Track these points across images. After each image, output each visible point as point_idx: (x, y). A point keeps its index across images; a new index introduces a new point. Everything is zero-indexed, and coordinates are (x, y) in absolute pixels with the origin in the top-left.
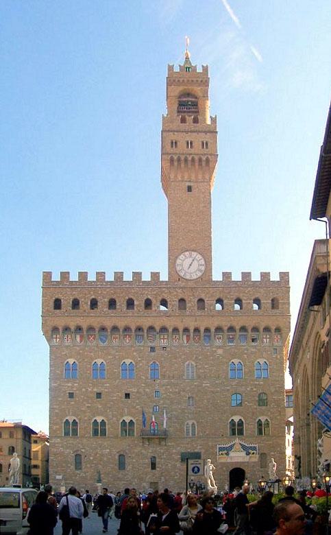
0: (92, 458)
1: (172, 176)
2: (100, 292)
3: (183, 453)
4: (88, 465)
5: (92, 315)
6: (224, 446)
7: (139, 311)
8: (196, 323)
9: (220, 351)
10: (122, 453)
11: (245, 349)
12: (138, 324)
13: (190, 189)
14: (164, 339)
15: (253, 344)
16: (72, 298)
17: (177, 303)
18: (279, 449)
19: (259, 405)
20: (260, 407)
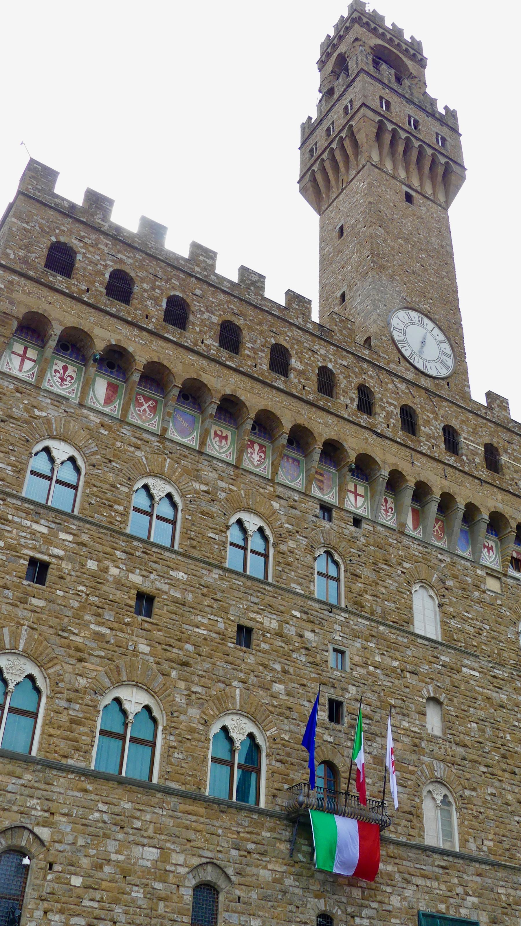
0: (77, 881)
2: (198, 292)
3: (424, 915)
7: (304, 389)
8: (446, 483)
9: (493, 584)
10: (209, 875)
12: (301, 420)
13: (409, 198)
14: (356, 494)
17: (398, 411)
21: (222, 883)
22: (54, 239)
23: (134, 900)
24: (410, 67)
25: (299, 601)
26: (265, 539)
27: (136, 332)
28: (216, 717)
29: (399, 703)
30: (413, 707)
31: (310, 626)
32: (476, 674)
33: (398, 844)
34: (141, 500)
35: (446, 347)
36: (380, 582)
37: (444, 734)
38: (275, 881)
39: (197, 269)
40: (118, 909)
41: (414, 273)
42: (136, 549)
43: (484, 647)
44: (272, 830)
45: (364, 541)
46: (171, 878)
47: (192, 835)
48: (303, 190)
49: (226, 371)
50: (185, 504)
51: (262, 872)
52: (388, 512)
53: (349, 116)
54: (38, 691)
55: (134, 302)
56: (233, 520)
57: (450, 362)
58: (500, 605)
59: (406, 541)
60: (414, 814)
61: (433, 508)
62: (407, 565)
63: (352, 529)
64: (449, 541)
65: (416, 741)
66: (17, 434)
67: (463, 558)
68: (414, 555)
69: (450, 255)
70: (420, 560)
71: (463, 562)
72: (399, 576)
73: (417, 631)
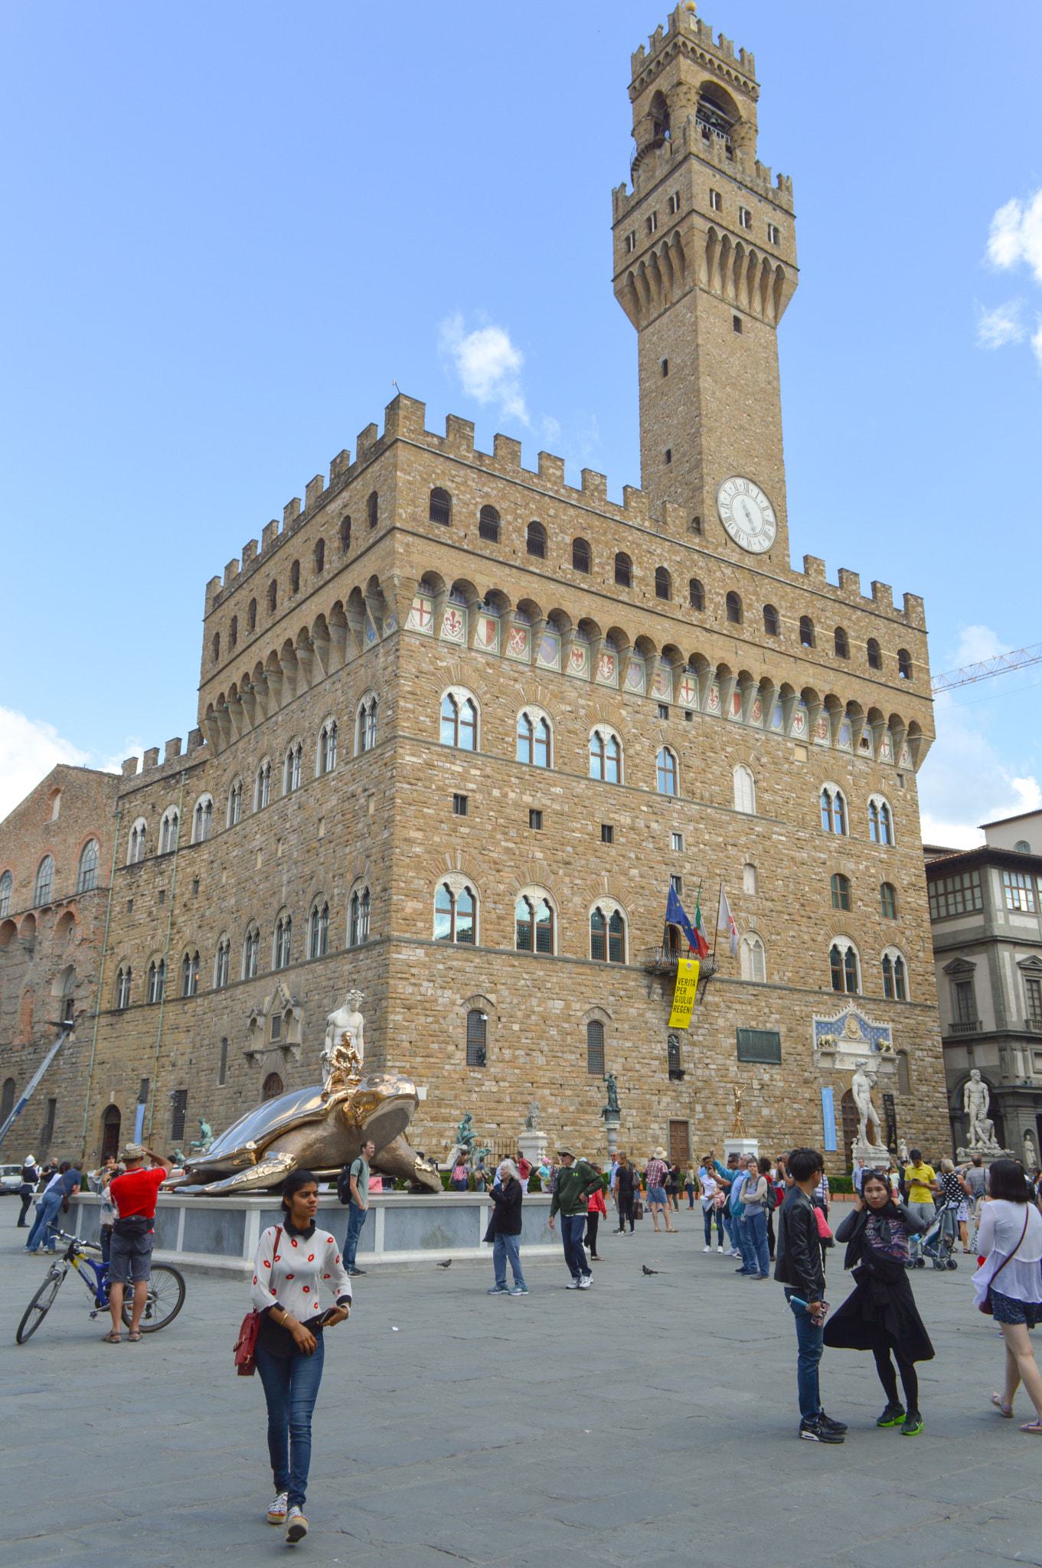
0: (516, 1027)
1: (703, 275)
2: (552, 512)
4: (506, 1052)
5: (532, 569)
6: (826, 1019)
8: (765, 667)
9: (800, 754)
10: (597, 1015)
11: (849, 762)
14: (688, 689)
15: (862, 751)
16: (481, 502)
18: (929, 1043)
19: (886, 915)
20: (885, 921)
21: (605, 1020)
22: (432, 487)
23: (552, 1036)
24: (740, 106)
25: (646, 797)
26: (617, 744)
27: (507, 570)
28: (591, 902)
29: (723, 872)
31: (654, 817)
33: (722, 981)
34: (522, 729)
35: (769, 515)
37: (757, 892)
38: (640, 1015)
39: (549, 485)
40: (543, 1043)
41: (741, 427)
42: (524, 773)
44: (635, 980)
46: (573, 1019)
47: (584, 989)
48: (619, 294)
49: (580, 593)
50: (555, 726)
51: (632, 1010)
53: (677, 218)
54: (472, 897)
55: (503, 537)
56: (592, 733)
57: (772, 531)
59: (729, 727)
60: (734, 957)
61: (754, 693)
62: (729, 749)
63: (685, 723)
64: (765, 721)
66: (427, 687)
69: (777, 392)
73: (738, 808)
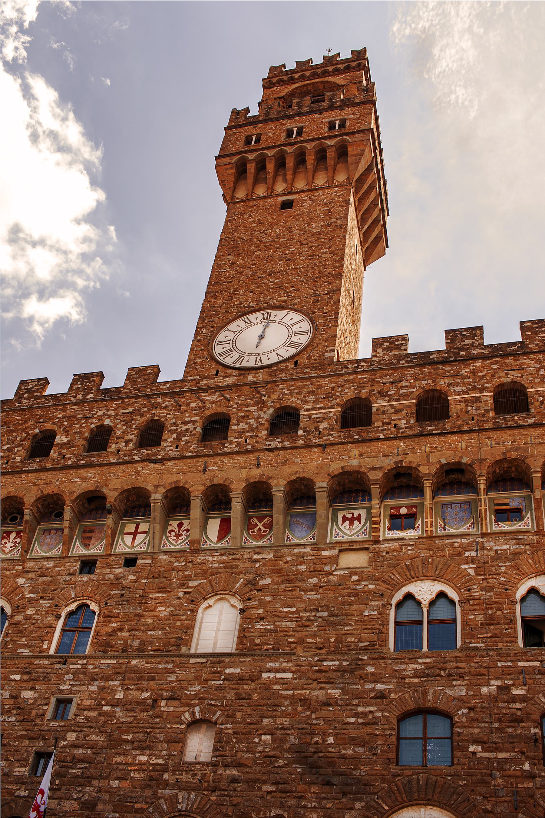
30: (162, 737)
32: (289, 675)
35: (306, 325)
36: (145, 614)
43: (309, 640)
45: (134, 578)
52: (182, 535)
58: (357, 581)
59: (200, 558)
63: (119, 571)
65: (152, 774)
67: (298, 546)
68: (211, 568)
70: (220, 570)
71: (296, 551)
72: (179, 598)
